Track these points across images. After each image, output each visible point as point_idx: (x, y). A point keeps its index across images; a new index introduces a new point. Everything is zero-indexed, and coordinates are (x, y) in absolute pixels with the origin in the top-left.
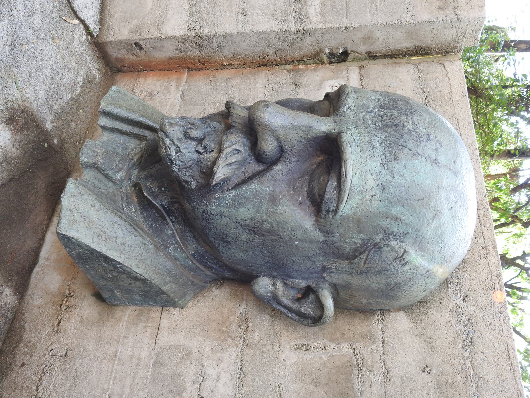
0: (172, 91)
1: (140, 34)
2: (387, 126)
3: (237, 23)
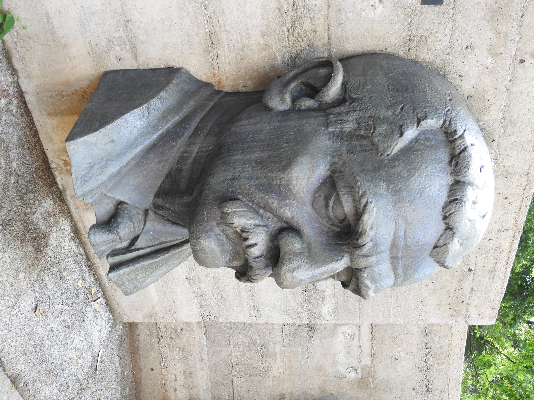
0: (195, 329)
1: (155, 319)
3: (250, 316)
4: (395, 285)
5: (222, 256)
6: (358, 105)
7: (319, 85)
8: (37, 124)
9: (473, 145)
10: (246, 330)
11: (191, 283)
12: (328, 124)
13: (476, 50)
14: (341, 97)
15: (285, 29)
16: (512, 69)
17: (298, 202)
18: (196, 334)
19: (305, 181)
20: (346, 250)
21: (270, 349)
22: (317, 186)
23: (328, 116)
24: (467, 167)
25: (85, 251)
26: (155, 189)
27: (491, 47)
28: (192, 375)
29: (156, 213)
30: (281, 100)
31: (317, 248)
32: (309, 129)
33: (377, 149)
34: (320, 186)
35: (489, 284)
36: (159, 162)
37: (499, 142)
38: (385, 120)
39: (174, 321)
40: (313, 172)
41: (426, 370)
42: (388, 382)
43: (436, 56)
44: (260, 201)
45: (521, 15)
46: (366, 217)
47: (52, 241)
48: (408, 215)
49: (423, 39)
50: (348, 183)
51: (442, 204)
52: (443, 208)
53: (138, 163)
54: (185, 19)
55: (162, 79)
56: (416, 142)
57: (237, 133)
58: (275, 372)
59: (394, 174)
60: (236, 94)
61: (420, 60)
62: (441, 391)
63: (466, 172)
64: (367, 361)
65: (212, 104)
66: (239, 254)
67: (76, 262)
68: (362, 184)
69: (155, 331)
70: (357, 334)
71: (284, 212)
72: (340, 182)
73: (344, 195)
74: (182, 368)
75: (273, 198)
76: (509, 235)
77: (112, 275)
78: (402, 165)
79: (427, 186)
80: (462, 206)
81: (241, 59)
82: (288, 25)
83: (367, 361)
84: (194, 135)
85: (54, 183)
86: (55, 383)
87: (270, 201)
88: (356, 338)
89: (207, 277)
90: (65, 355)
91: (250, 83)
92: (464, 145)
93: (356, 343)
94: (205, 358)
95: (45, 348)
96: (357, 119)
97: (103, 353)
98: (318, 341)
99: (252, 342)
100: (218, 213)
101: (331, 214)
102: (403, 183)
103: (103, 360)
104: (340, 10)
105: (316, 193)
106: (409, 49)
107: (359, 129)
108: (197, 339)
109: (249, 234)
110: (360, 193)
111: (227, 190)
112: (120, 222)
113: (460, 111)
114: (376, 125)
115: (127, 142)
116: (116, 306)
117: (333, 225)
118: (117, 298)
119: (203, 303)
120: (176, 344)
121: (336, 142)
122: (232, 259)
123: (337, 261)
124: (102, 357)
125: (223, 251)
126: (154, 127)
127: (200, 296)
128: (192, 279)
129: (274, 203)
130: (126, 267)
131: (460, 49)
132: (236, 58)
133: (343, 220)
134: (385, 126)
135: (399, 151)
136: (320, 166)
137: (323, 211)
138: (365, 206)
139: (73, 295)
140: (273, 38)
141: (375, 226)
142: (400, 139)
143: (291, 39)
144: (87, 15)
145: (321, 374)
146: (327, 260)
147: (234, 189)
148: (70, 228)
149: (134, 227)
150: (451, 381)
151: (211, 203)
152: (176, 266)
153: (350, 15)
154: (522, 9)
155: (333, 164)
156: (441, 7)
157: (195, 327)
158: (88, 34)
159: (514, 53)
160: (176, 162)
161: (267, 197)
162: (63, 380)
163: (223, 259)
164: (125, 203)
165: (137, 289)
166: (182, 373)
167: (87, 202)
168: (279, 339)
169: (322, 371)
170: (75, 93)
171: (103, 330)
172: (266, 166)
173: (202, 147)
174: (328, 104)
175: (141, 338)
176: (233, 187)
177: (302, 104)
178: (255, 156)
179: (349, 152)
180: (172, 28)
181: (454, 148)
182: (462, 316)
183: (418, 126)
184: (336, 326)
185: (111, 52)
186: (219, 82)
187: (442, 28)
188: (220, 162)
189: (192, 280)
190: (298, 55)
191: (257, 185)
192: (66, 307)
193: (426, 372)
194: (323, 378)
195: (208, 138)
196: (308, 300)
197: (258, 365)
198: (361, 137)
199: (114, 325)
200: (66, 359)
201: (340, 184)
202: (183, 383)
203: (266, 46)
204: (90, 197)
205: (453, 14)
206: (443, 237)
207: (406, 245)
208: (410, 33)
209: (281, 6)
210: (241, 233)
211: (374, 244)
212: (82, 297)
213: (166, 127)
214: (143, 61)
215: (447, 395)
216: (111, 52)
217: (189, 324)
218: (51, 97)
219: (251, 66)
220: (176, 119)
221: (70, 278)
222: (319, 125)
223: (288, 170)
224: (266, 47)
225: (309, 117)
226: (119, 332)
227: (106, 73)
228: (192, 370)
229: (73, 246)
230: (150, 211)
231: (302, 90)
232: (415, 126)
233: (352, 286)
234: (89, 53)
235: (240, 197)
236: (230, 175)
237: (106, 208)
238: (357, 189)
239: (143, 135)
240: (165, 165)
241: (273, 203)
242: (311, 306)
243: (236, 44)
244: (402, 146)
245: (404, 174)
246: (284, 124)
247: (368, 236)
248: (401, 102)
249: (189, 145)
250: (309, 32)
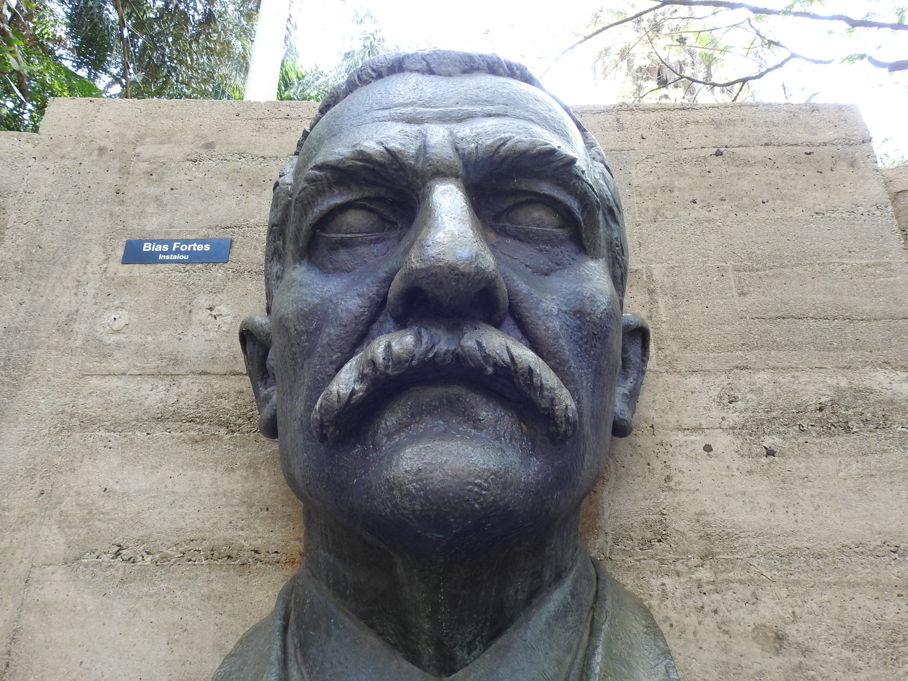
36: (329, 635)
44: (327, 360)
54: (178, 599)
81: (267, 509)
82: (223, 431)
104: (213, 358)
132: (264, 519)
180: (188, 627)
203: (250, 466)
209: (190, 439)
219: (282, 494)
224: (253, 467)
243: (239, 515)
250: (239, 402)
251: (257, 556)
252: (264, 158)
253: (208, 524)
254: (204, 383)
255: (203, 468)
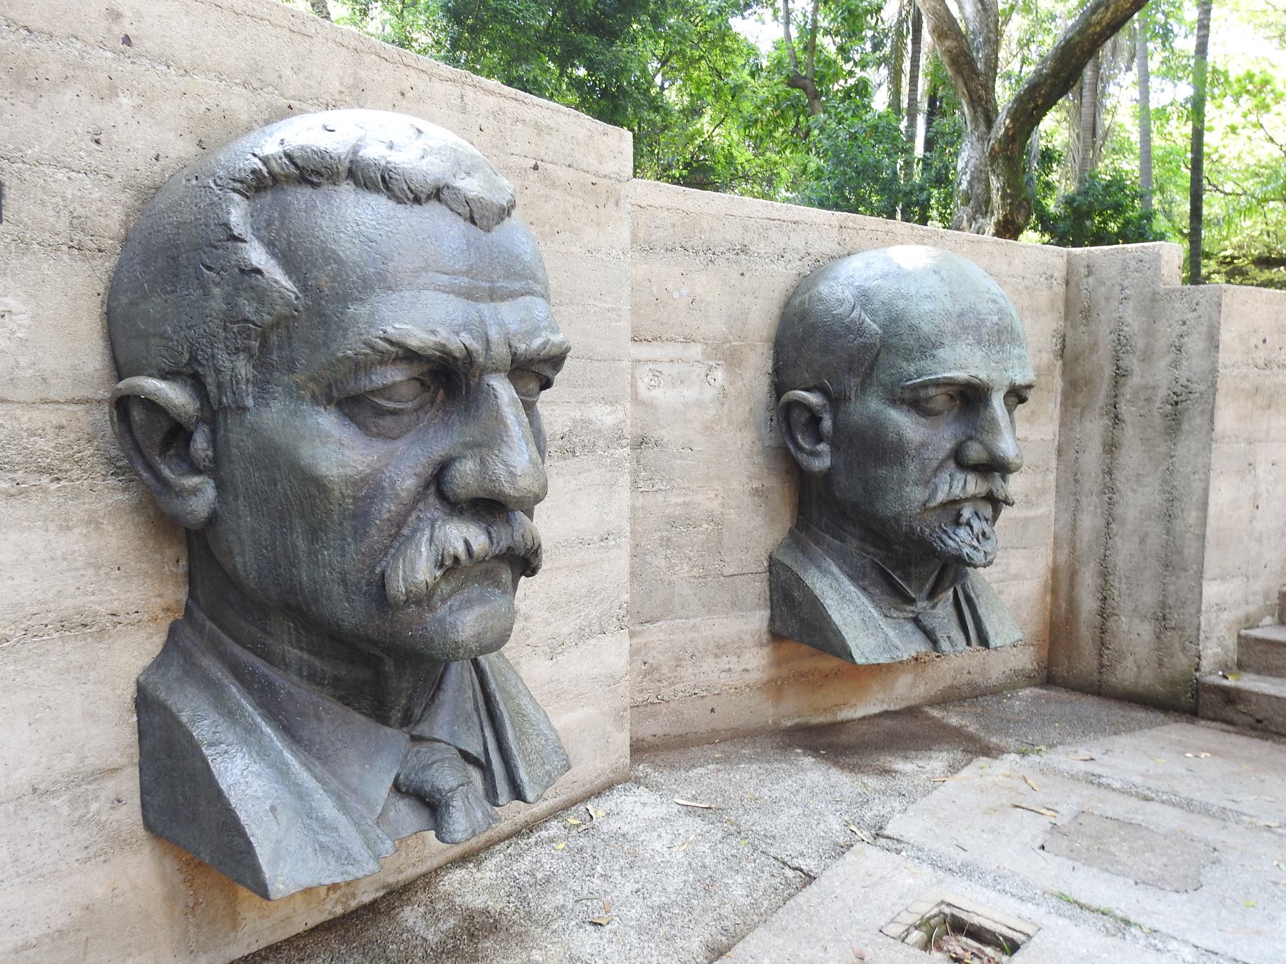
0: (644, 641)
1: (625, 710)
2: (999, 340)
3: (619, 546)
4: (545, 296)
5: (491, 601)
6: (202, 350)
7: (164, 423)
8: (254, 948)
9: (282, 142)
10: (645, 554)
11: (560, 650)
12: (239, 408)
13: (102, 124)
14: (189, 382)
15: (55, 486)
16: (144, 61)
17: (388, 464)
18: (652, 639)
19: (347, 453)
20: (477, 380)
21: (677, 513)
22: (357, 430)
23: (225, 408)
24: (322, 154)
25: (504, 840)
26: (373, 725)
27: (96, 96)
28: (722, 643)
29: (419, 721)
30: (196, 495)
31: (472, 432)
32: (249, 442)
33: (287, 317)
34: (357, 424)
35: (562, 137)
36: (319, 719)
37: (293, 98)
38: (230, 300)
39: (628, 677)
40: (328, 435)
41: (710, 253)
42: (730, 316)
43: (115, 202)
44: (386, 533)
45: (26, 32)
46: (413, 343)
47: (478, 902)
48: (411, 267)
49: (77, 223)
50: (350, 373)
51: (391, 204)
52: (400, 203)
53: (319, 759)
55: (157, 718)
56: (274, 246)
57: (259, 578)
58: (715, 504)
59: (333, 288)
60: (191, 578)
61: (123, 231)
62: (746, 229)
63: (331, 157)
64: (696, 350)
65: (209, 624)
66: (486, 572)
67: (520, 855)
68: (349, 347)
69: (648, 709)
70: (651, 365)
71: (407, 490)
72: (348, 388)
73: (371, 381)
74: (710, 660)
75: (380, 511)
76: (472, 95)
77: (530, 796)
78: (315, 273)
79: (356, 229)
80: (395, 168)
82: (45, 480)
83: (696, 350)
84: (267, 656)
85: (372, 907)
86: (725, 880)
87: (386, 516)
88: (659, 367)
89: (548, 624)
90: (680, 865)
91: (169, 552)
92: (281, 158)
93: (665, 368)
94: (692, 621)
95: (667, 901)
96: (229, 354)
97: (682, 797)
98: (664, 432)
99: (666, 543)
100: (410, 610)
101: (410, 405)
102: (350, 273)
103: (694, 796)
104: (11, 380)
105: (371, 431)
106: (100, 251)
107: (247, 349)
108: (661, 636)
109: (446, 555)
110: (368, 351)
111: (365, 594)
112: (432, 786)
113: (218, 161)
114: (240, 318)
115: (277, 783)
116: (603, 779)
117: (432, 403)
118: (587, 779)
119: (596, 628)
120: (670, 672)
121: (273, 393)
122: (497, 584)
123: (496, 397)
124: (688, 799)
125: (482, 600)
126: (250, 731)
127: (583, 635)
128: (553, 648)
129: (388, 509)
130: (518, 772)
131: (100, 155)
133: (423, 384)
134: (241, 301)
135: (290, 278)
136: (318, 423)
137: (406, 419)
138: (391, 343)
139: (578, 857)
140: (73, 509)
141: (431, 327)
142: (267, 275)
143: (76, 473)
144: (21, 872)
145: (718, 428)
146: (495, 414)
147: (363, 581)
148: (458, 871)
149: (442, 760)
150: (729, 213)
151: (391, 623)
152: (522, 680)
153: (23, 361)
154: (12, 29)
155: (315, 400)
156: (7, 184)
157: (639, 640)
158: (62, 866)
159: (109, 54)
160: (319, 688)
161: (378, 522)
162: (721, 866)
163: (498, 602)
164: (396, 779)
165: (559, 749)
166: (718, 660)
167: (391, 851)
168: (660, 497)
169: (714, 425)
170: (190, 882)
171: (642, 800)
172: (320, 524)
173: (291, 641)
174: (202, 405)
175: (660, 732)
176: (359, 583)
177: (203, 455)
178: (301, 544)
179: (291, 370)
180: (50, 704)
181: (287, 176)
182: (618, 186)
183: (243, 241)
184: (636, 400)
185: (103, 819)
186: (168, 610)
187: (54, 186)
188: (313, 608)
189: (555, 649)
190: (111, 461)
191: (355, 539)
192: (599, 868)
193: (714, 254)
194: (724, 425)
195: (273, 630)
196: (590, 448)
197: (703, 533)
198: (264, 347)
199: (637, 781)
200: (687, 863)
201: (352, 387)
202: (734, 659)
203: (89, 522)
204: (382, 847)
205: (24, 162)
206: (454, 206)
207: (467, 273)
208: (65, 248)
210: (444, 569)
211: (465, 330)
212: (582, 841)
213: (250, 708)
214: (121, 756)
215: (752, 221)
216: (103, 819)
217: (634, 653)
218: (198, 926)
220: (234, 690)
221: (549, 864)
222: (242, 422)
223: (326, 482)
224: (93, 521)
225: (227, 441)
226: (649, 770)
227: (148, 825)
228: (712, 644)
229: (491, 863)
230: (414, 733)
231: (177, 455)
232: (243, 245)
233: (547, 372)
234: (105, 862)
235: (378, 570)
236: (337, 590)
237: (406, 815)
238: (359, 357)
239: (263, 752)
240: (324, 710)
241: (389, 511)
242: (601, 443)
243: (86, 579)
244: (280, 271)
245: (332, 270)
246: (241, 489)
247: (448, 339)
248: (197, 270)
249: (286, 665)
250: (61, 441)
251: (115, 619)
252: (30, 32)
253: (50, 595)
254: (5, 415)
255: (30, 528)
